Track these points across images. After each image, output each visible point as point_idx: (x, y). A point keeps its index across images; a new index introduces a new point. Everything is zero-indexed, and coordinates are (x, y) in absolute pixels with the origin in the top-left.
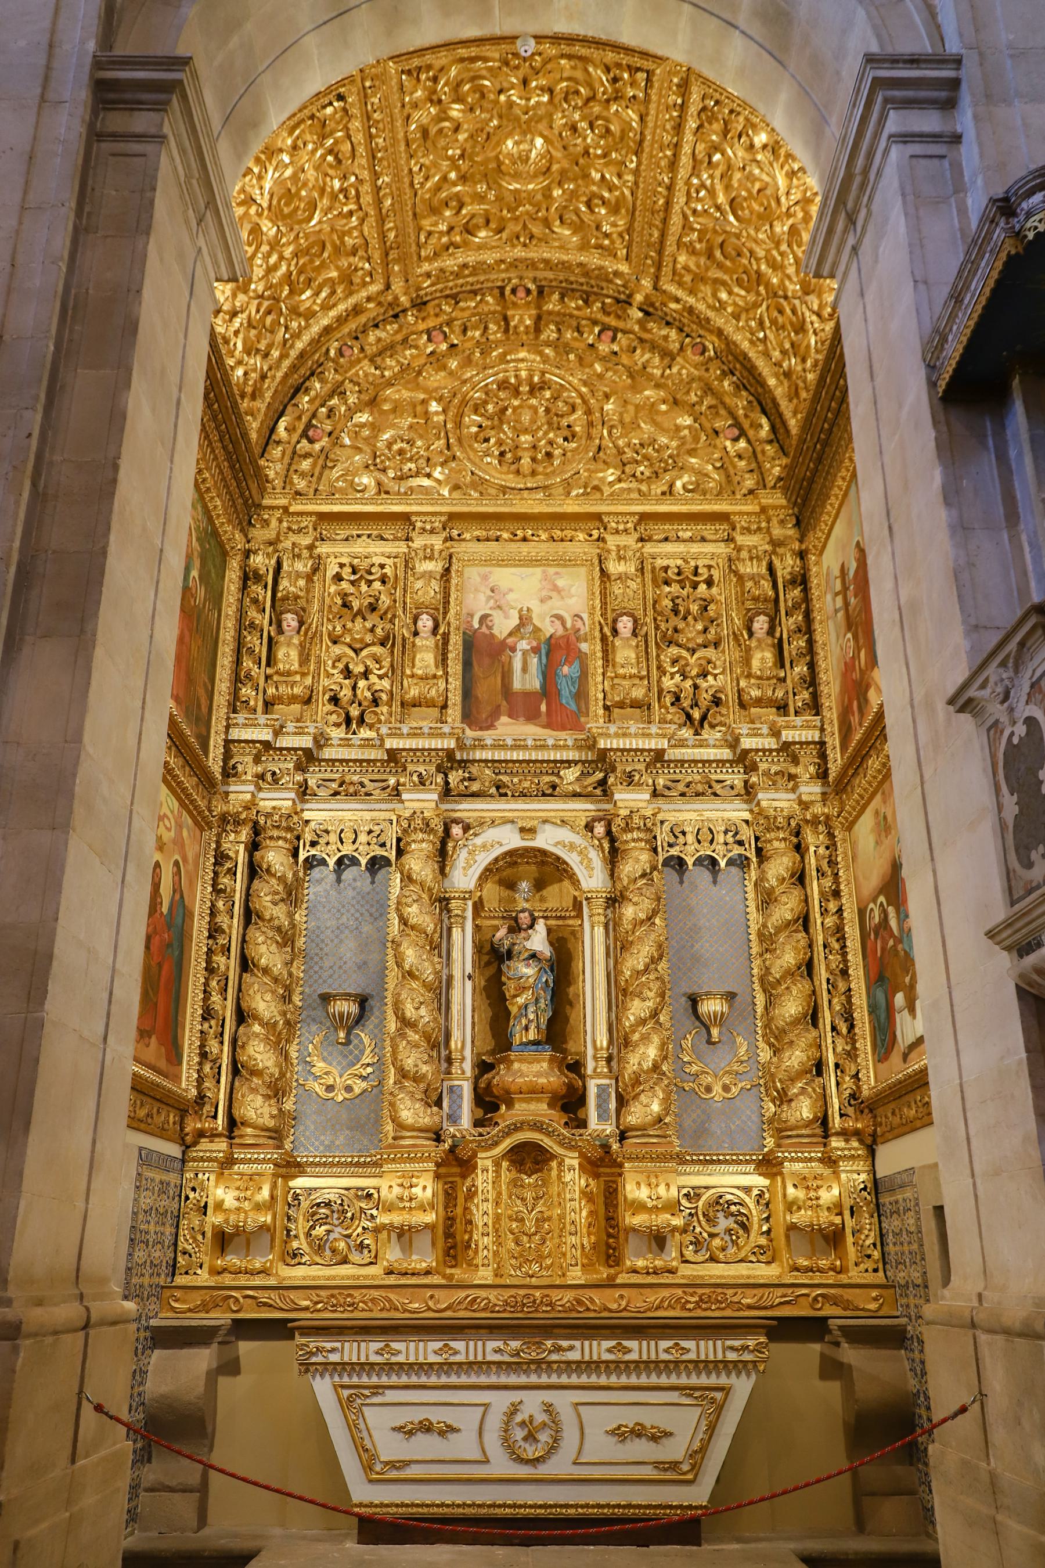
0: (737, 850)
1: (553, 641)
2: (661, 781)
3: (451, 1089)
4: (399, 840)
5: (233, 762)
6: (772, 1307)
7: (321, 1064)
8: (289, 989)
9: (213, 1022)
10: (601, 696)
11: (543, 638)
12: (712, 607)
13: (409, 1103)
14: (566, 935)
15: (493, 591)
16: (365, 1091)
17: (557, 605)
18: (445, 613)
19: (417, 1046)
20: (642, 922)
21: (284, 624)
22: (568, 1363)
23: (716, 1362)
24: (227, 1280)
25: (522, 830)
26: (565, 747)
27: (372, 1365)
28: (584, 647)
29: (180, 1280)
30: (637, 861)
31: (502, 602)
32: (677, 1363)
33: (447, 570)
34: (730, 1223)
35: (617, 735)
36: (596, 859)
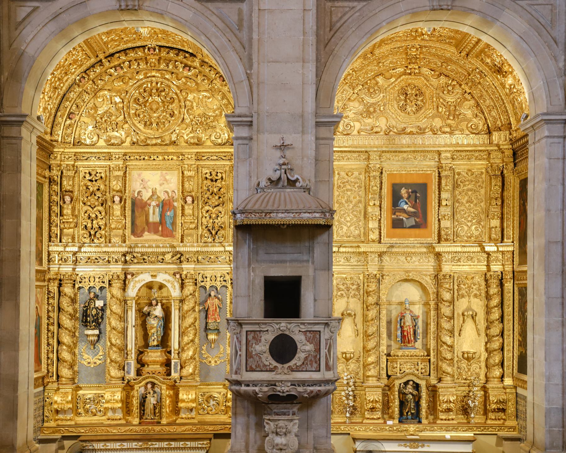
0: (224, 283)
2: (200, 258)
3: (128, 363)
4: (109, 281)
5: (51, 257)
6: (217, 430)
7: (86, 355)
8: (74, 333)
9: (50, 347)
10: (180, 225)
11: (160, 201)
12: (222, 190)
13: (113, 371)
14: (169, 306)
16: (100, 364)
17: (166, 187)
18: (125, 192)
19: (116, 352)
20: (190, 311)
21: (66, 200)
22: (155, 448)
23: (195, 448)
24: (60, 423)
25: (152, 276)
26: (167, 247)
27: (101, 449)
28: (175, 204)
29: (46, 424)
30: (189, 290)
31: (146, 186)
32: (185, 448)
33: (125, 172)
34: (214, 403)
35: (183, 246)
36: (177, 286)
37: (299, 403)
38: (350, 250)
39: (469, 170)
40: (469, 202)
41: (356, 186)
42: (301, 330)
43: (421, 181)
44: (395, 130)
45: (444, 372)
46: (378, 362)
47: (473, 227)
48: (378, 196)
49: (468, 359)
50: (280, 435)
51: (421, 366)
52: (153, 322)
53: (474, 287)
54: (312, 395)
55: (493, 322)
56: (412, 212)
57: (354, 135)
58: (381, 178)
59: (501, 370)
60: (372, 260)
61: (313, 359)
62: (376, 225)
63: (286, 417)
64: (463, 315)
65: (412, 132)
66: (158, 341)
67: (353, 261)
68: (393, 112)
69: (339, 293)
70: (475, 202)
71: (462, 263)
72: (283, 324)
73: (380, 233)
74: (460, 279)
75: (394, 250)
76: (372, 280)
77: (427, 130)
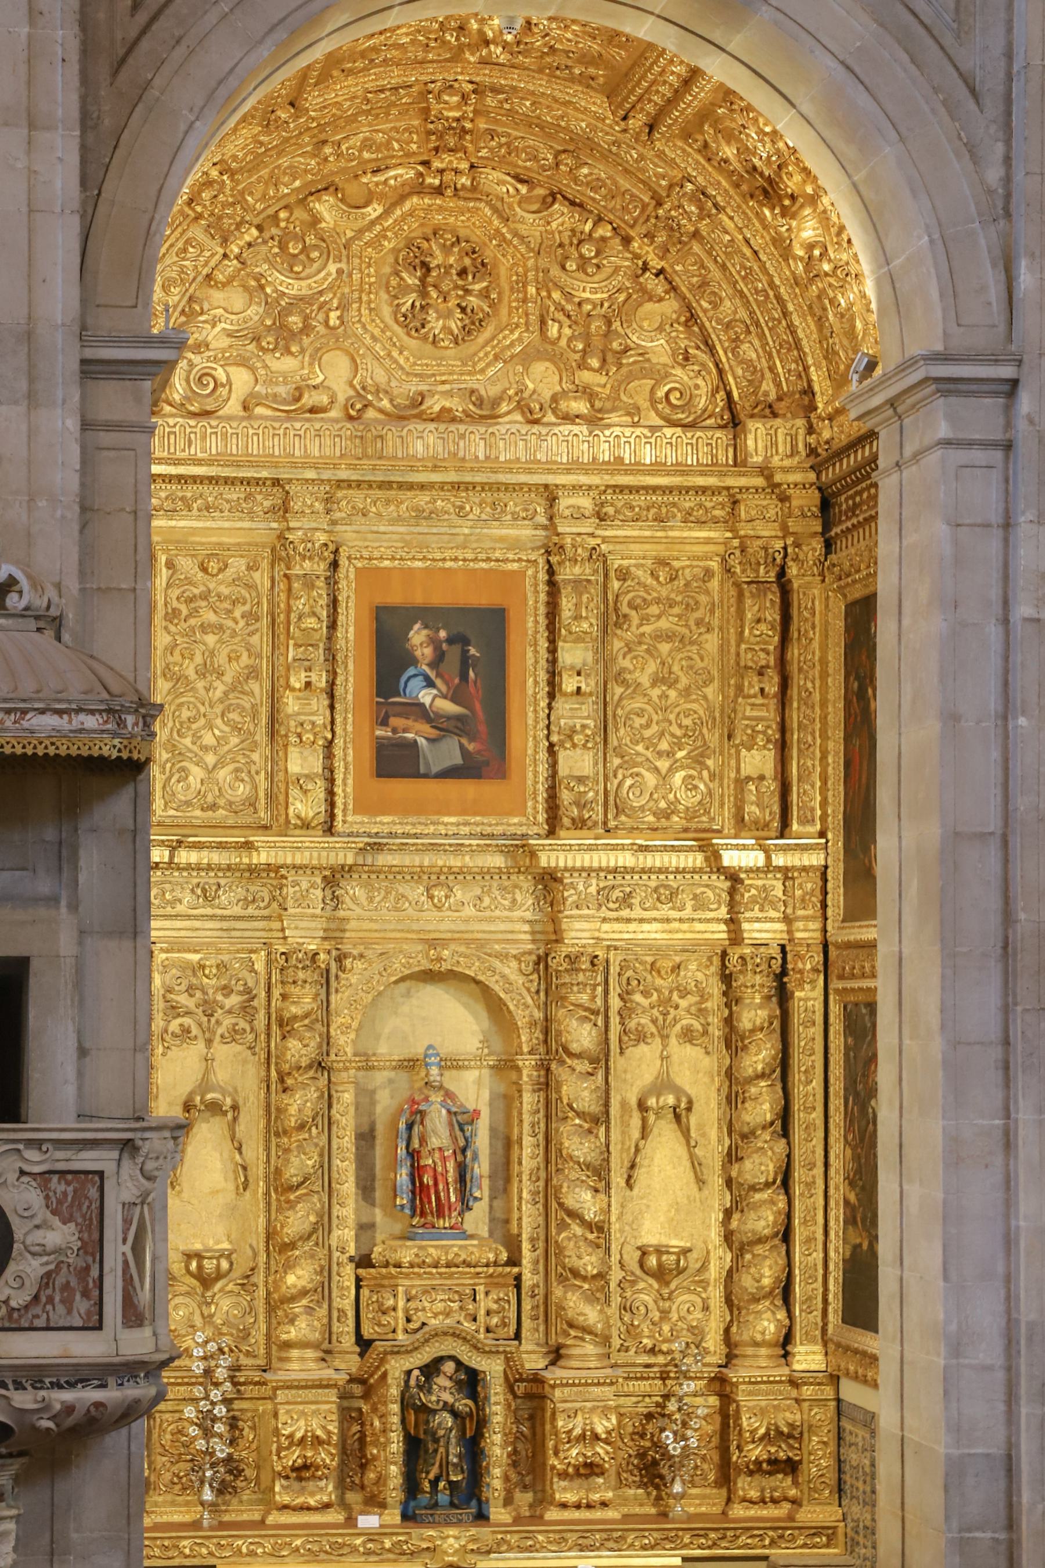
37: (21, 1454)
38: (216, 857)
39: (662, 562)
40: (663, 681)
41: (237, 614)
42: (27, 1168)
43: (482, 599)
44: (385, 403)
45: (571, 1325)
46: (323, 1290)
47: (678, 778)
48: (319, 655)
49: (661, 1274)
51: (485, 1303)
53: (683, 1003)
54: (70, 1421)
55: (753, 1133)
56: (449, 718)
57: (229, 418)
58: (332, 582)
59: (781, 1315)
60: (302, 899)
61: (74, 1283)
62: (316, 764)
64: (642, 1107)
65: (450, 410)
67: (230, 900)
68: (377, 332)
69: (174, 1026)
70: (684, 681)
71: (637, 913)
73: (331, 793)
74: (630, 973)
75: (384, 859)
76: (301, 975)
77: (504, 408)
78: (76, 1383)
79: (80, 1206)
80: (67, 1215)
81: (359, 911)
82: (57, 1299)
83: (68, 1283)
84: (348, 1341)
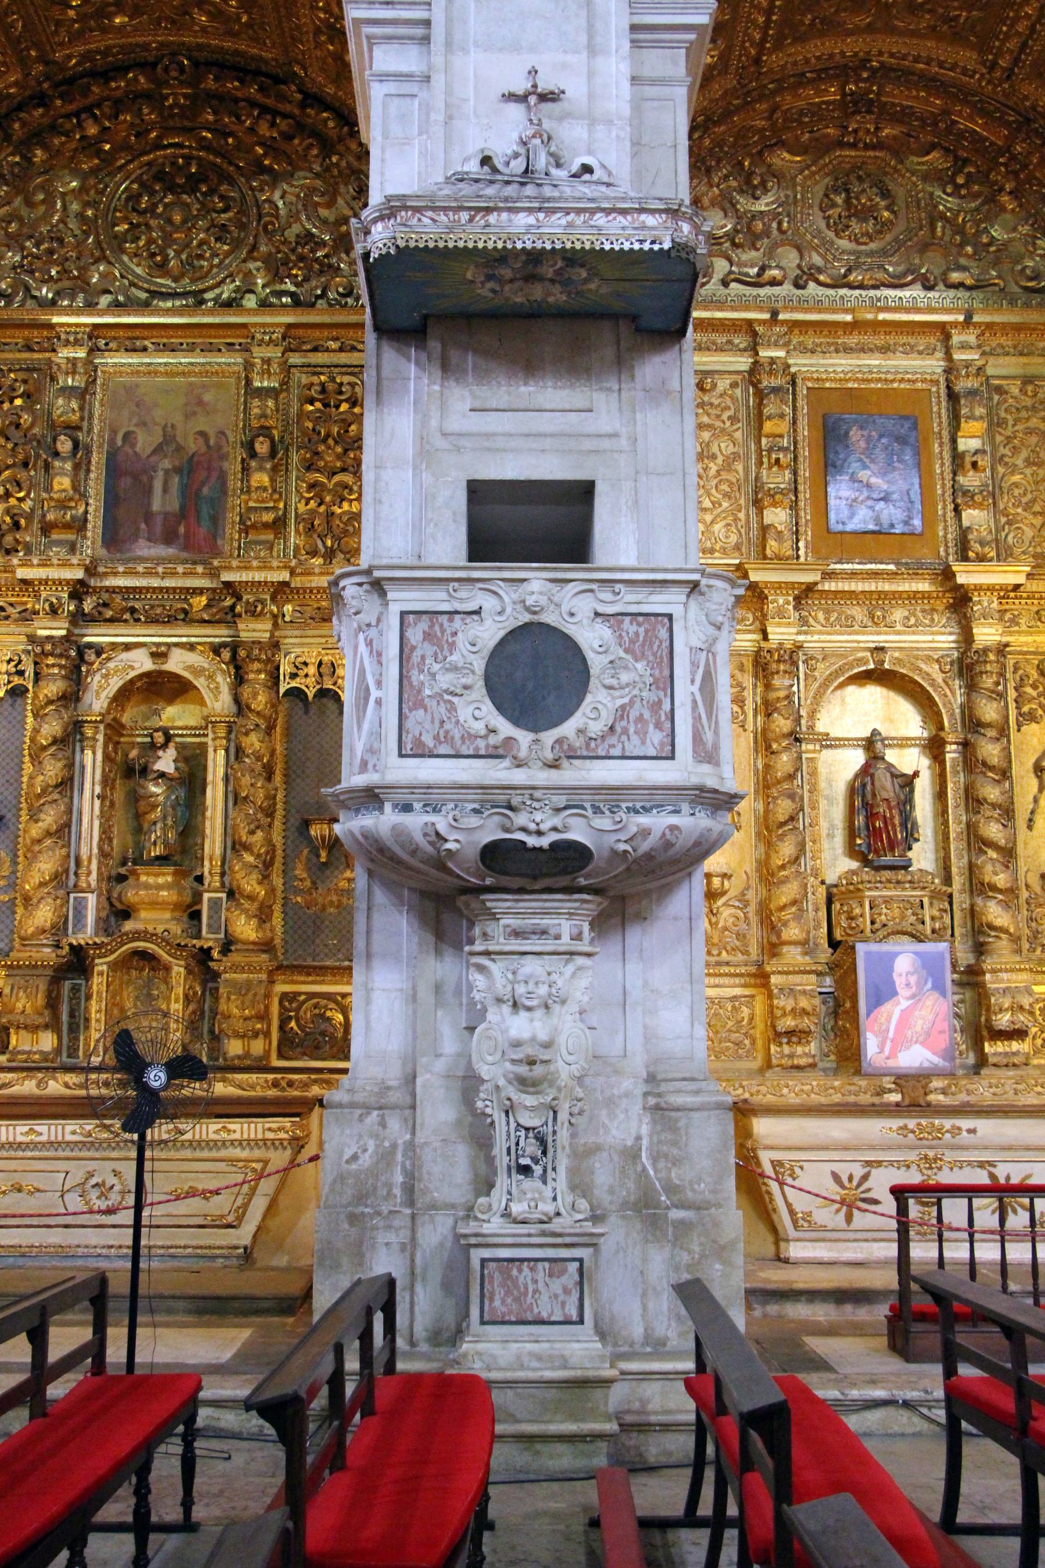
1: (196, 459)
15: (138, 405)
17: (202, 423)
36: (224, 682)
40: (1034, 464)
41: (725, 417)
50: (529, 1009)
52: (154, 789)
54: (645, 846)
61: (647, 715)
63: (549, 945)
66: (166, 844)
72: (536, 586)
78: (652, 808)
79: (651, 647)
80: (639, 654)
81: (820, 628)
82: (632, 730)
83: (641, 715)
84: (824, 942)
